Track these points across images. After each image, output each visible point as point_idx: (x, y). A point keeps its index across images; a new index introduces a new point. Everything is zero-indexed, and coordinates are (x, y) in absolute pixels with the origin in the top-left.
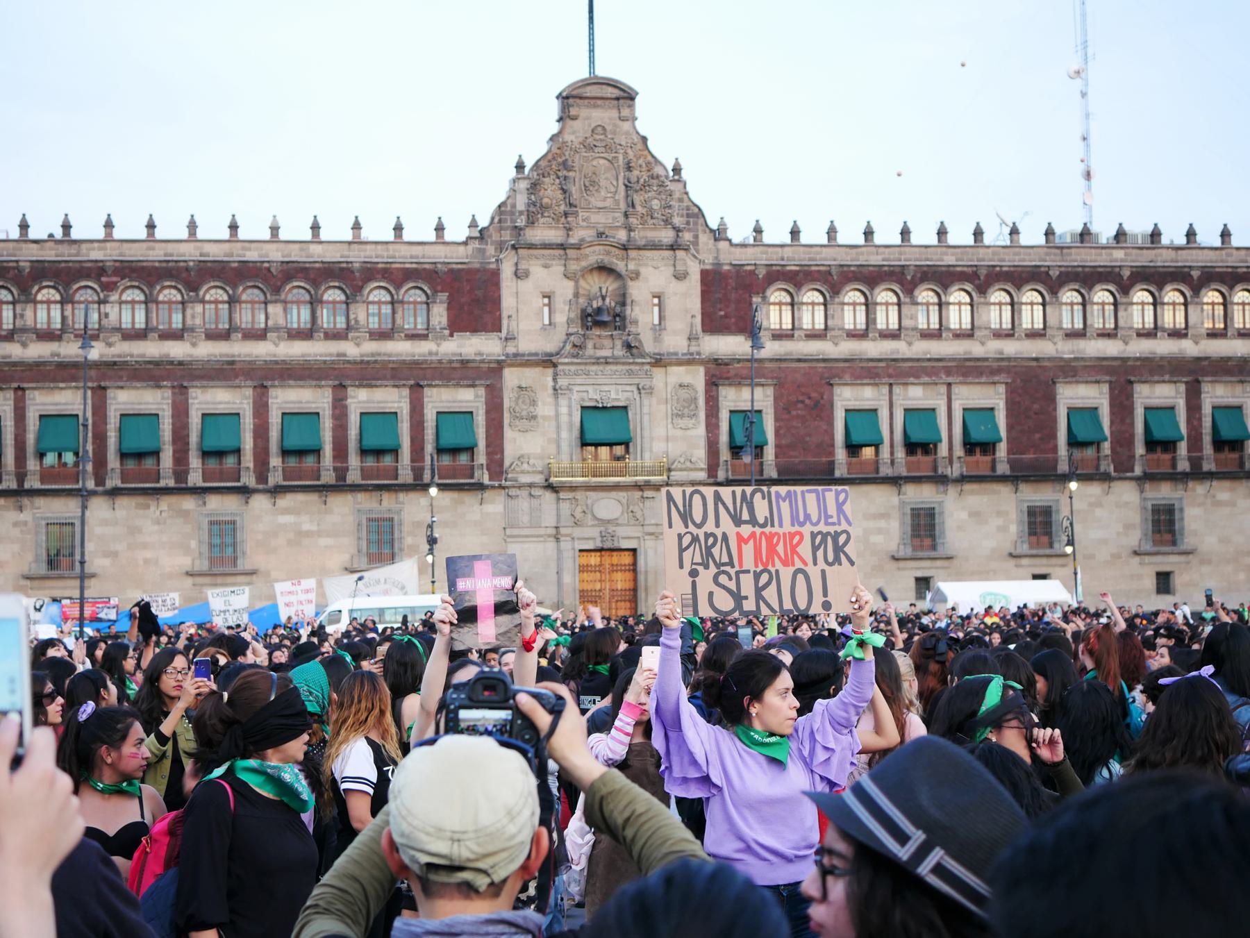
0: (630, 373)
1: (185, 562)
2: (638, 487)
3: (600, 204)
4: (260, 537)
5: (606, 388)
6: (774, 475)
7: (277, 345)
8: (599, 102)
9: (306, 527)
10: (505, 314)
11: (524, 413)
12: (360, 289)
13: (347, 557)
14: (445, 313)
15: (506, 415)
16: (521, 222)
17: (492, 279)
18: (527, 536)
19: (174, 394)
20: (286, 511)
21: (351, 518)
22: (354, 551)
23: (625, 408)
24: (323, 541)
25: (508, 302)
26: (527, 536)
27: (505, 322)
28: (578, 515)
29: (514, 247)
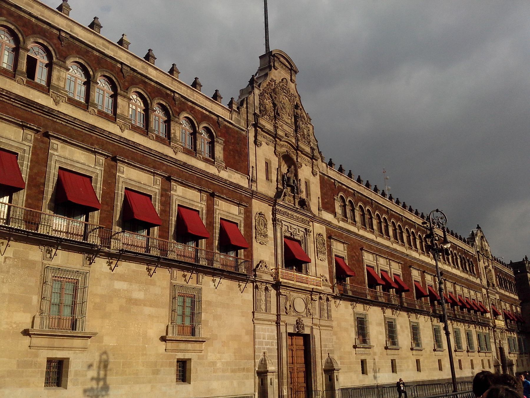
0: (303, 221)
1: (24, 320)
2: (312, 292)
3: (286, 120)
4: (98, 300)
5: (295, 227)
6: (350, 293)
7: (122, 131)
8: (284, 67)
9: (138, 295)
10: (251, 165)
11: (262, 232)
12: (179, 114)
13: (164, 327)
14: (222, 152)
15: (254, 231)
16: (257, 111)
17: (245, 140)
18: (264, 320)
19: (36, 139)
20: (122, 278)
21: (168, 292)
22: (166, 321)
23: (299, 241)
24: (148, 310)
25: (252, 158)
26: (264, 320)
27: (251, 169)
28: (288, 307)
29: (255, 126)
